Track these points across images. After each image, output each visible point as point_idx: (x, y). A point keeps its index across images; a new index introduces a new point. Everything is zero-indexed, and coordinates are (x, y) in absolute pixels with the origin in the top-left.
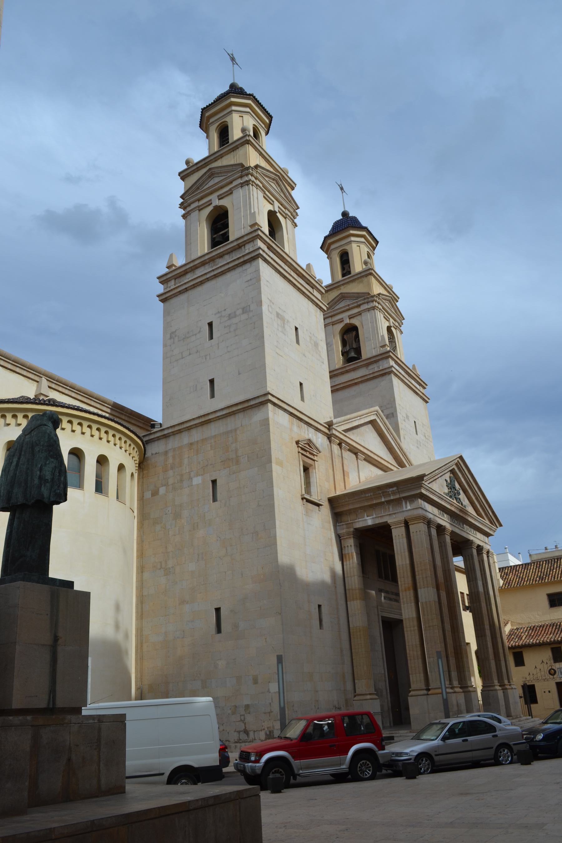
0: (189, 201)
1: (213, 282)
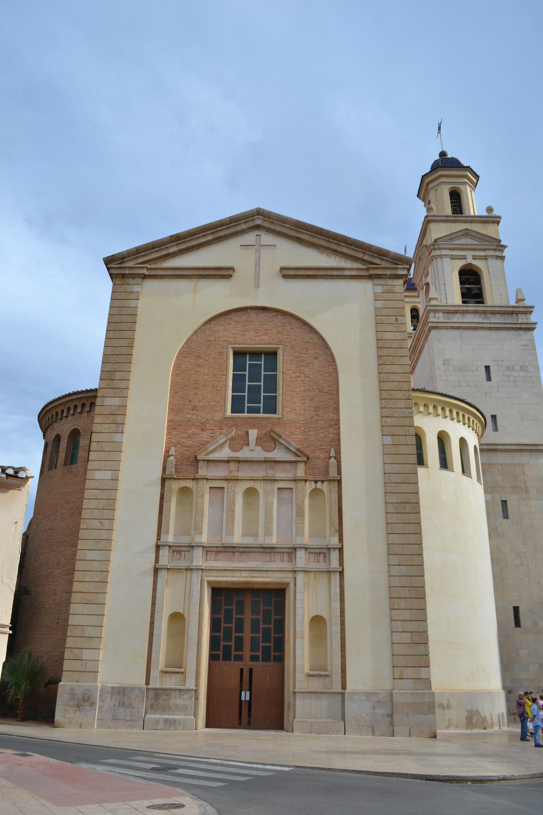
1: (487, 332)
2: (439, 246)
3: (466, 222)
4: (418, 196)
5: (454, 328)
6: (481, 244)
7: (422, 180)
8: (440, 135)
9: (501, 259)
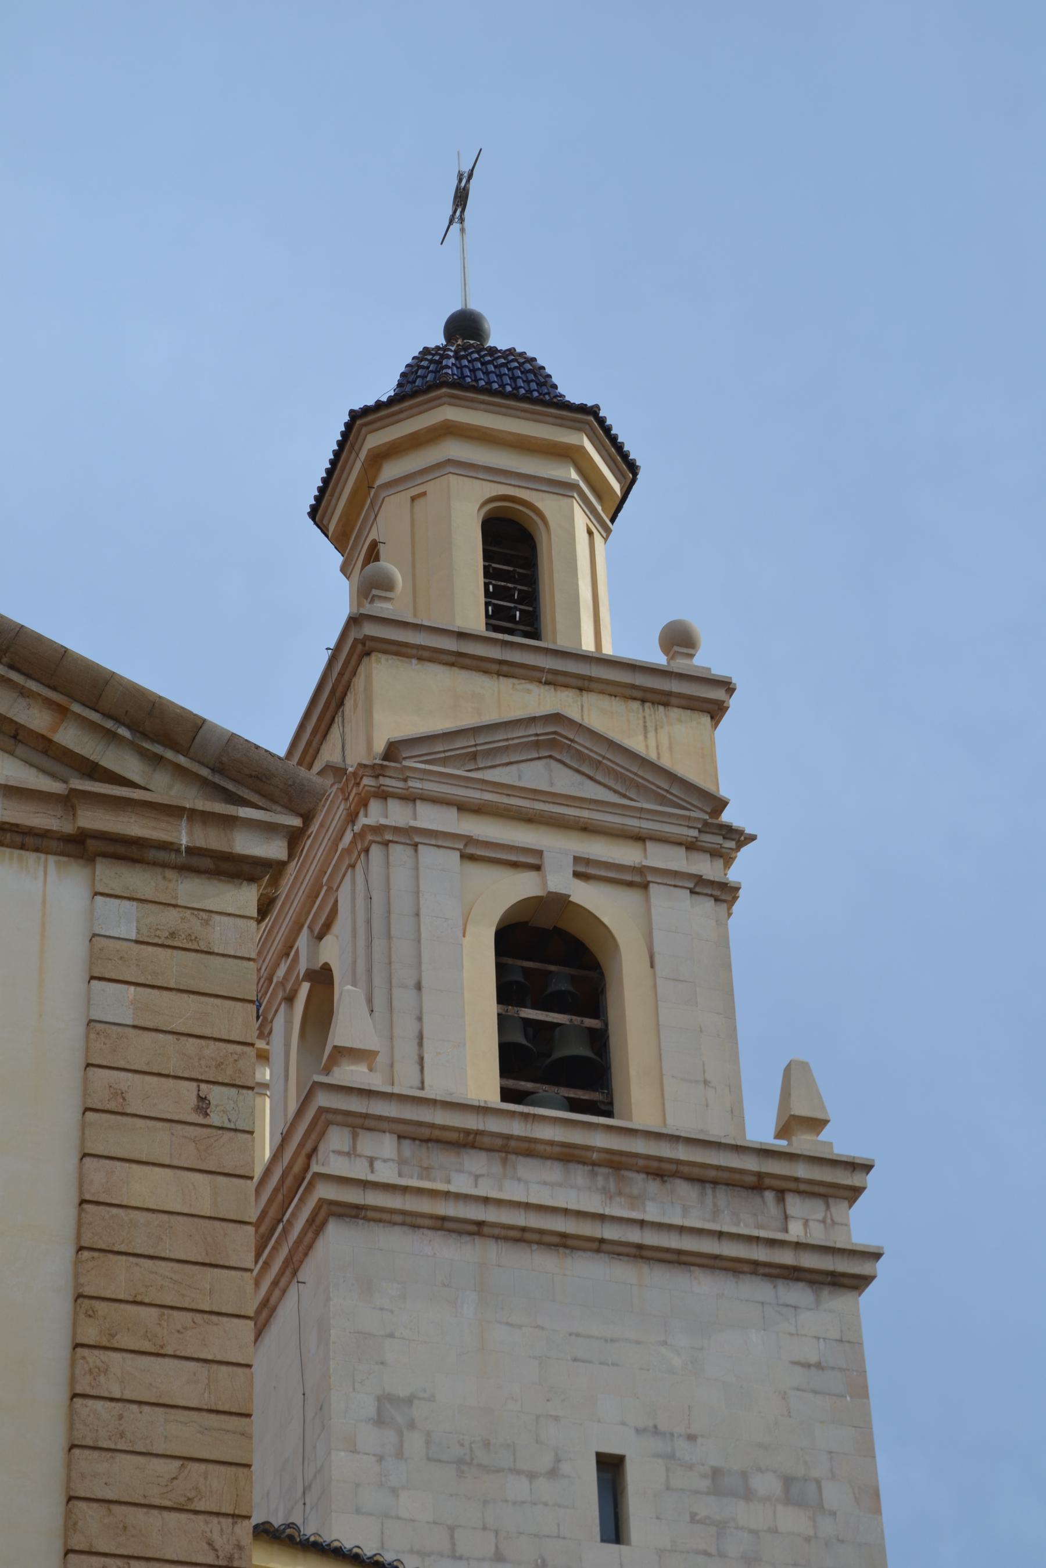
0: (418, 785)
2: (405, 780)
3: (554, 680)
4: (313, 513)
5: (448, 1225)
6: (624, 806)
7: (345, 435)
8: (463, 230)
9: (717, 900)
